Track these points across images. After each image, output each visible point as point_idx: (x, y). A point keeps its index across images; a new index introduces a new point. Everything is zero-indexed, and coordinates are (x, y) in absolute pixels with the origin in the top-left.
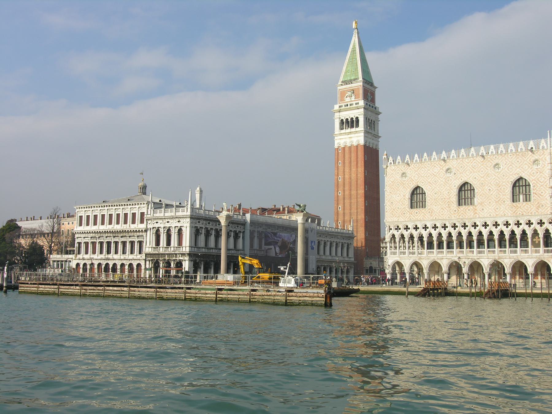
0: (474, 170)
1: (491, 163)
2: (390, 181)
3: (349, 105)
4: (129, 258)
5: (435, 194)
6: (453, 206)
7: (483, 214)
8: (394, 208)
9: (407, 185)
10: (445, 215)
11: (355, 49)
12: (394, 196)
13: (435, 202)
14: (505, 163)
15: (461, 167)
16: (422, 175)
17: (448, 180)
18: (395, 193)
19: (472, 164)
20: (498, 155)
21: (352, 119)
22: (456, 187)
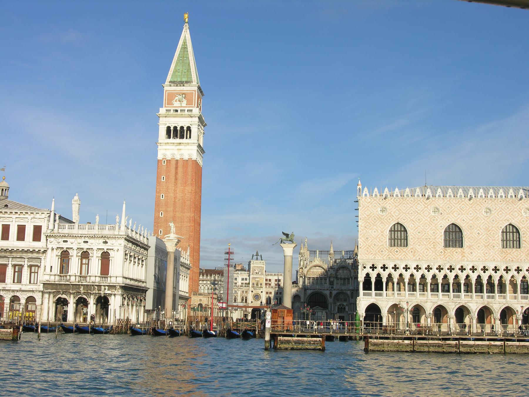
0: (462, 212)
1: (480, 206)
2: (365, 214)
3: (179, 111)
4: (12, 289)
5: (419, 232)
6: (439, 247)
7: (472, 258)
8: (369, 245)
9: (386, 221)
10: (430, 255)
11: (186, 46)
13: (419, 242)
14: (495, 208)
15: (448, 207)
16: (404, 211)
17: (434, 220)
18: (370, 228)
20: (488, 200)
21: (182, 128)
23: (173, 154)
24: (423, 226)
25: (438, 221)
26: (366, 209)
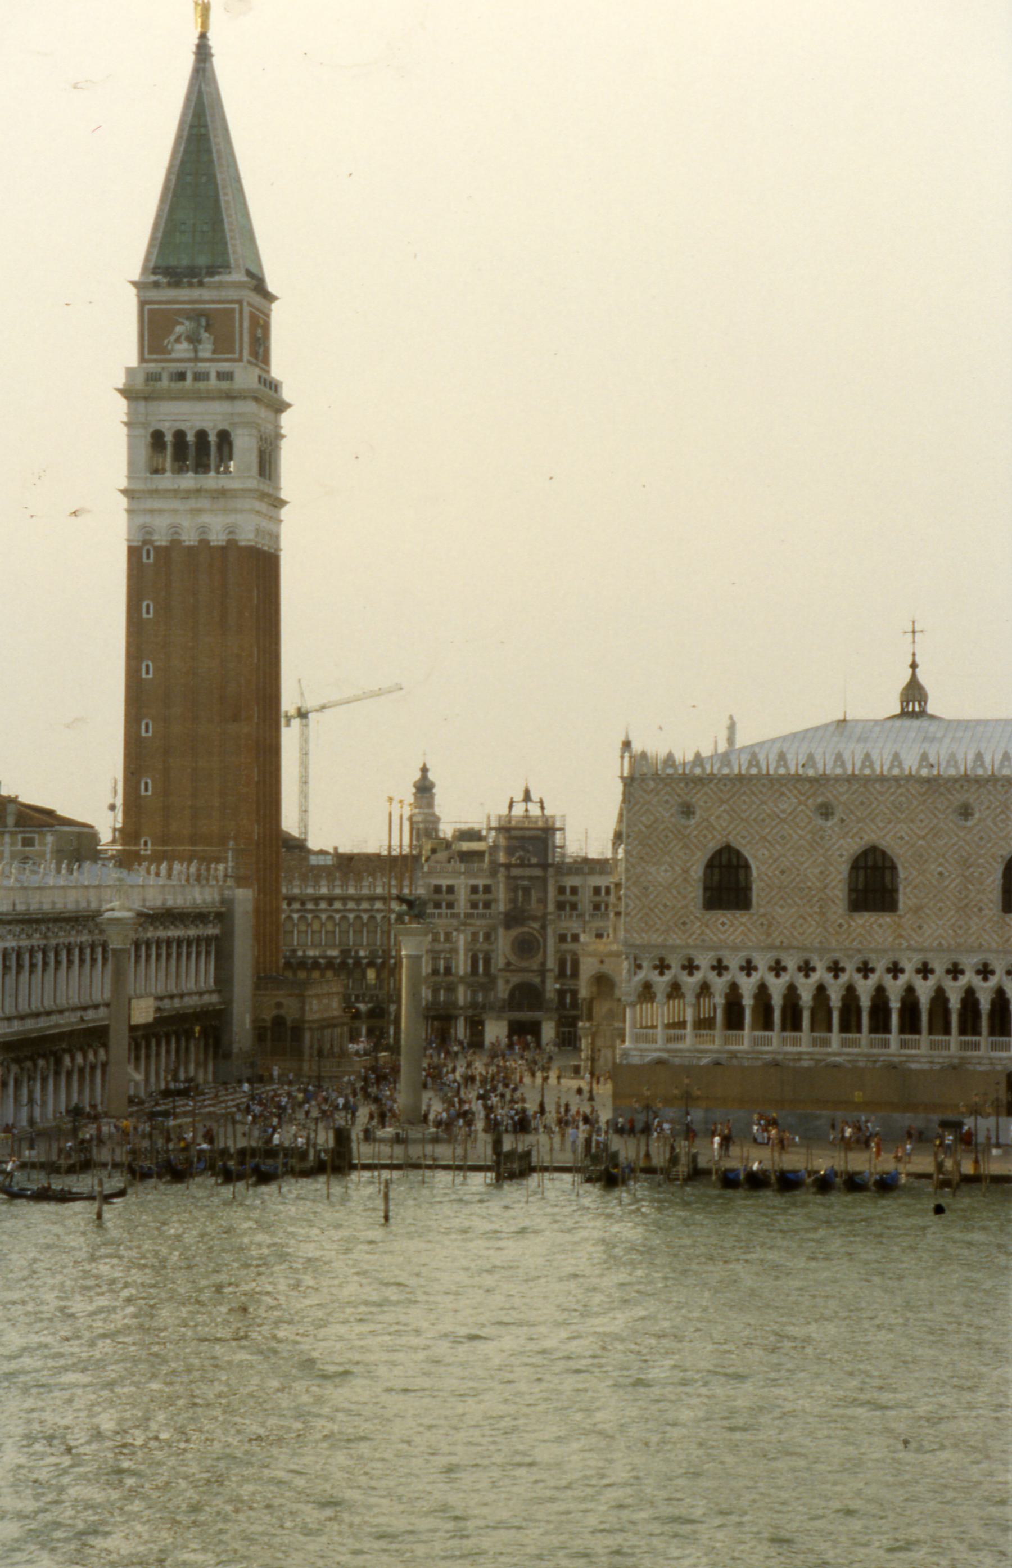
0: (899, 814)
1: (948, 799)
2: (641, 822)
3: (189, 376)
5: (783, 872)
6: (835, 913)
7: (920, 940)
8: (652, 905)
9: (695, 841)
10: (811, 934)
11: (203, 131)
12: (653, 870)
14: (987, 804)
16: (744, 816)
19: (892, 798)
22: (844, 859)
23: (175, 529)
24: (793, 855)
25: (834, 840)
26: (645, 808)
